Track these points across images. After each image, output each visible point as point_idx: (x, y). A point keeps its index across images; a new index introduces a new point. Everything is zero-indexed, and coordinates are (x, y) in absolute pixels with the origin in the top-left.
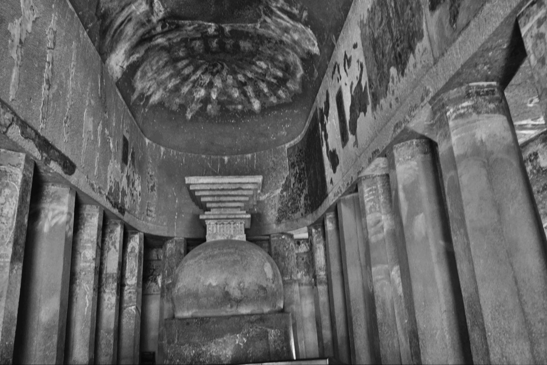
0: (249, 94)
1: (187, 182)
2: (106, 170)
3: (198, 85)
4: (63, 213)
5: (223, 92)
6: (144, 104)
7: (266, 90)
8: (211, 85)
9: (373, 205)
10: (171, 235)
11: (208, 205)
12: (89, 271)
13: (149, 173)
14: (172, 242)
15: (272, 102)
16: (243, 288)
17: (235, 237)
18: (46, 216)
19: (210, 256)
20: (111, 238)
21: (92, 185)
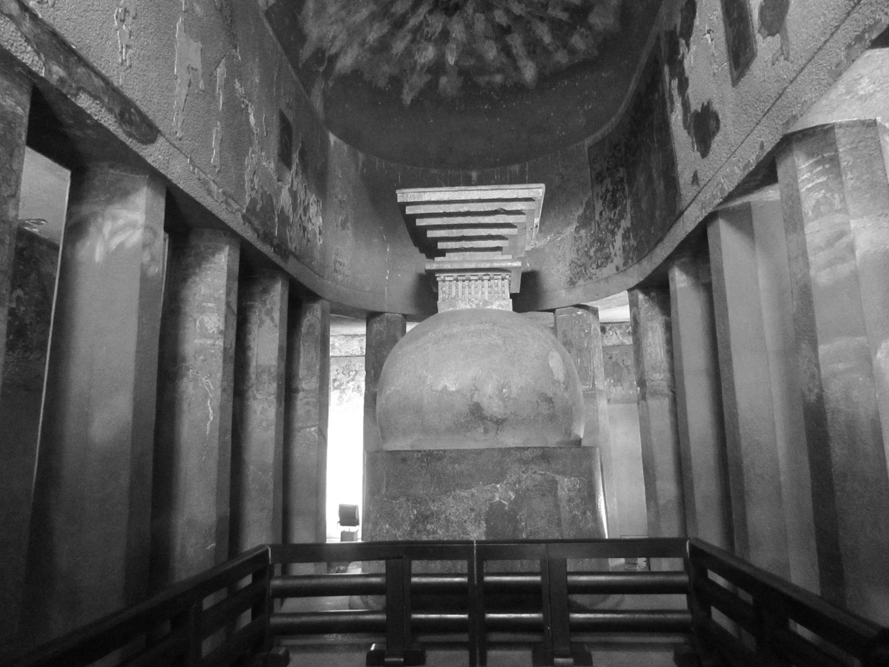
0: (515, 51)
1: (400, 199)
2: (241, 166)
3: (422, 36)
4: (133, 225)
5: (468, 50)
6: (324, 71)
7: (547, 39)
8: (445, 35)
9: (825, 197)
10: (378, 309)
11: (441, 245)
12: (213, 355)
13: (336, 197)
14: (382, 320)
15: (558, 62)
16: (508, 397)
17: (492, 304)
18: (100, 230)
19: (445, 336)
20: (265, 302)
21: (204, 183)
